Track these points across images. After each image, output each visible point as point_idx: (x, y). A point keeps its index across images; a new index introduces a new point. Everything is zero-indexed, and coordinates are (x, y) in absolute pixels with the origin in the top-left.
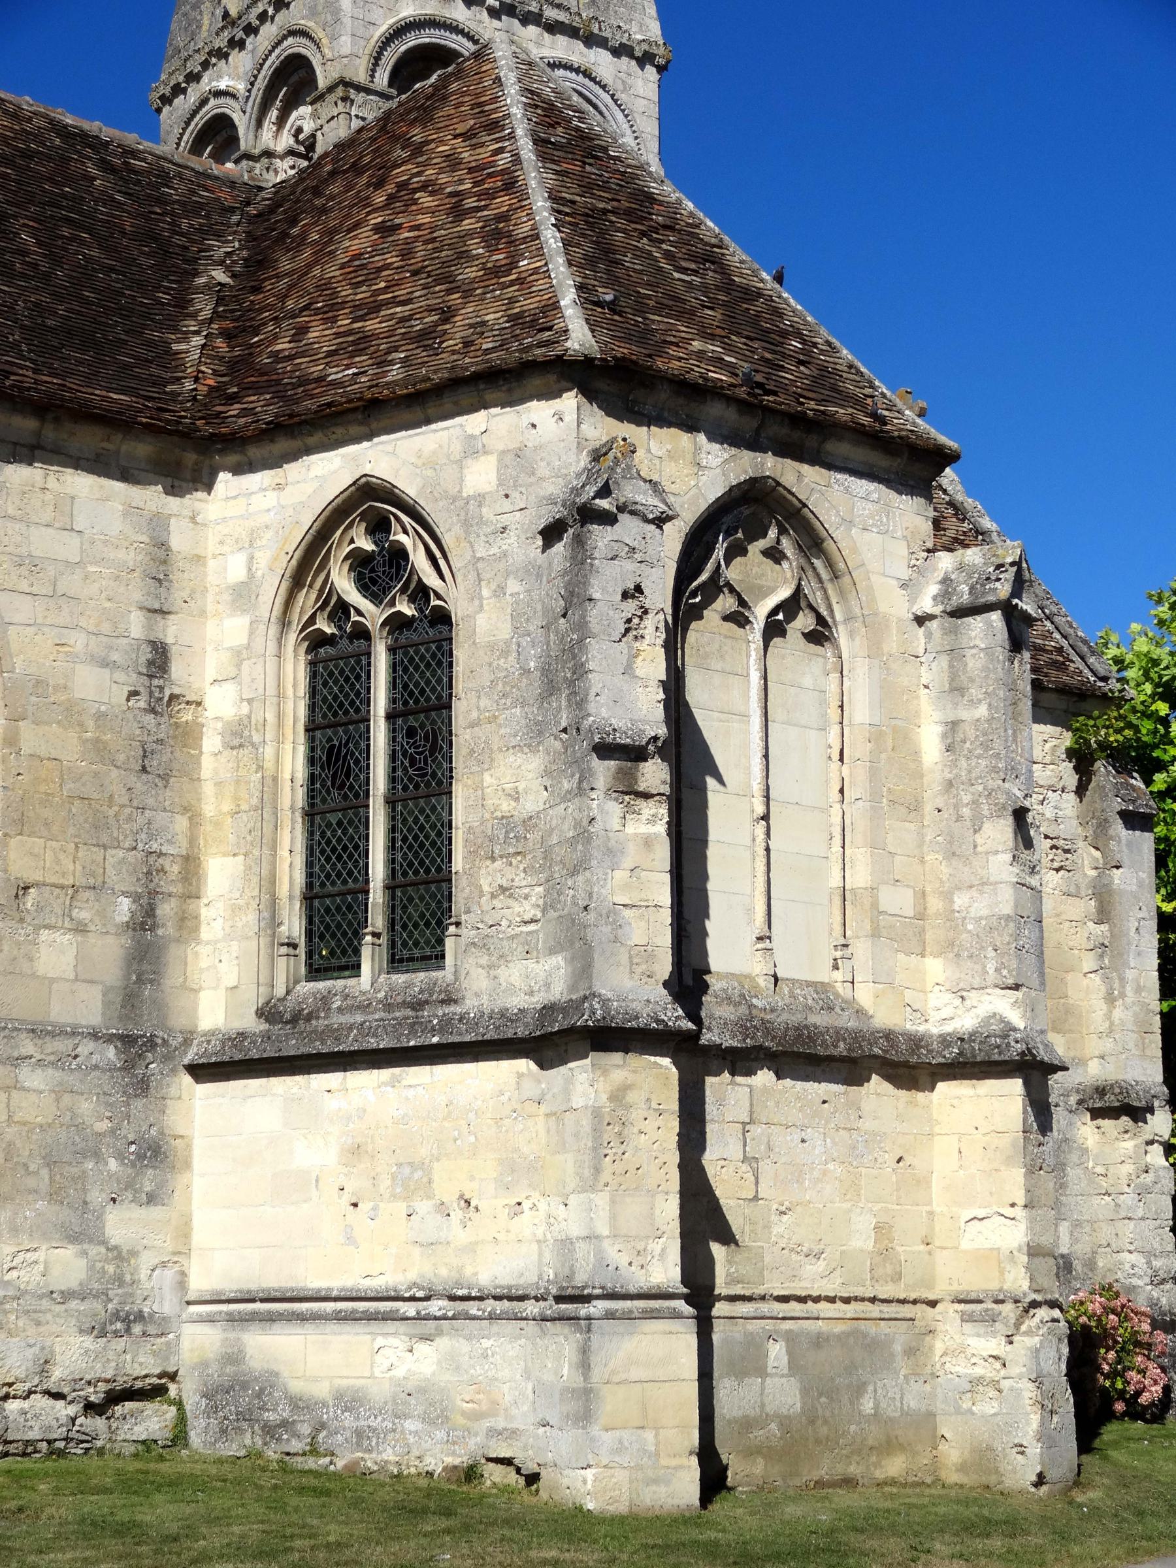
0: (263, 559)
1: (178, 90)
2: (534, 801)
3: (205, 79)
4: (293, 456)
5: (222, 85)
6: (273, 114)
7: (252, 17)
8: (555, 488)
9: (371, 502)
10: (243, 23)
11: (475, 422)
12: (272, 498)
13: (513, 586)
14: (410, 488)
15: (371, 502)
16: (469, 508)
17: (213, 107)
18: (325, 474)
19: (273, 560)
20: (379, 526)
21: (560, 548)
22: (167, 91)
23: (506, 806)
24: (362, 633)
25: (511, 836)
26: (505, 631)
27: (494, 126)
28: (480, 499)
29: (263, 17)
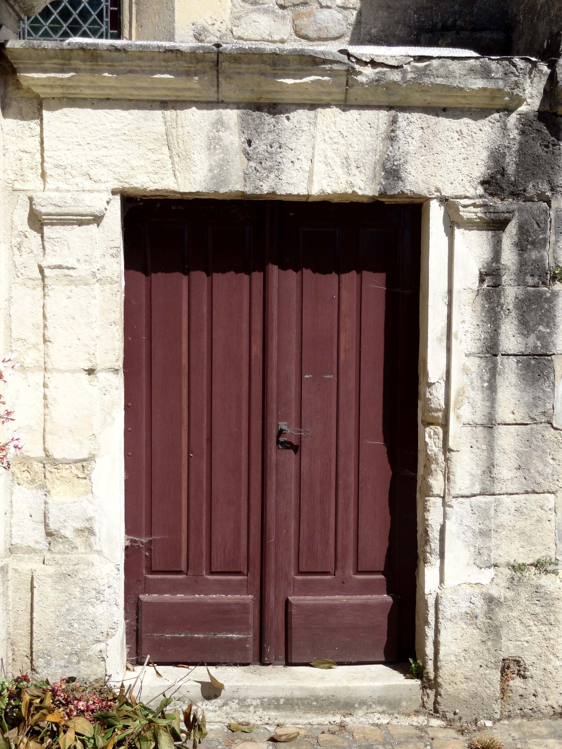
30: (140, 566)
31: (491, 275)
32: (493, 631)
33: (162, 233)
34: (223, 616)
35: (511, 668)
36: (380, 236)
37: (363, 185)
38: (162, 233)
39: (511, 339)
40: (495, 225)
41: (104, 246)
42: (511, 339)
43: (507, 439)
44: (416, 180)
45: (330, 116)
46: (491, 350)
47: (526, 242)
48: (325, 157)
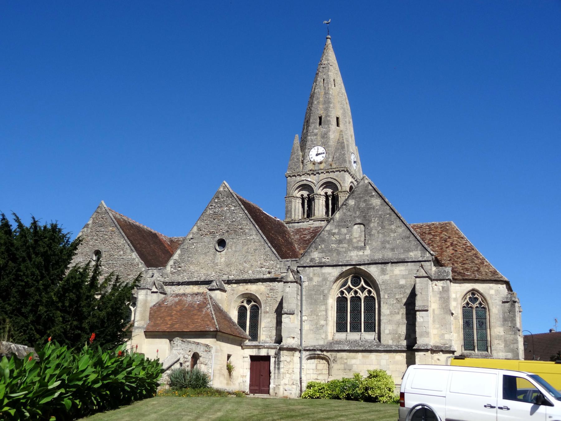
0: (458, 296)
1: (295, 176)
2: (502, 333)
3: (303, 176)
4: (463, 283)
5: (309, 180)
6: (321, 188)
7: (320, 172)
8: (503, 296)
9: (473, 292)
10: (317, 171)
11: (491, 285)
12: (459, 288)
13: (498, 307)
14: (481, 291)
15: (473, 292)
16: (491, 296)
17: (305, 182)
18: (469, 286)
19: (460, 296)
20: (473, 294)
21: (507, 305)
22: (291, 175)
23: (498, 334)
24: (471, 307)
25: (499, 337)
26: (497, 312)
27: (462, 238)
28: (492, 295)
29: (322, 173)
30: (251, 385)
31: (275, 361)
32: (274, 390)
33: (253, 358)
34: (256, 390)
35: (276, 393)
36: (267, 358)
37: (266, 354)
38: (253, 358)
39: (277, 366)
40: (275, 357)
41: (248, 360)
42: (277, 366)
43: (276, 374)
44: (269, 354)
45: (264, 349)
46: (275, 367)
47: (278, 359)
48: (263, 352)
